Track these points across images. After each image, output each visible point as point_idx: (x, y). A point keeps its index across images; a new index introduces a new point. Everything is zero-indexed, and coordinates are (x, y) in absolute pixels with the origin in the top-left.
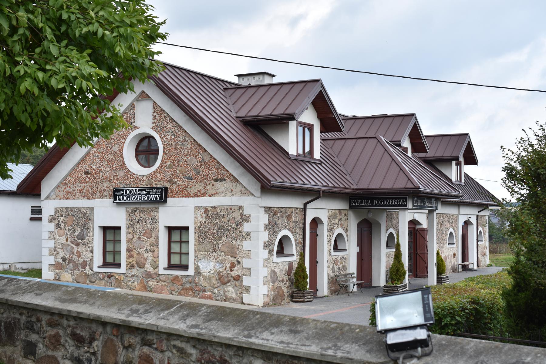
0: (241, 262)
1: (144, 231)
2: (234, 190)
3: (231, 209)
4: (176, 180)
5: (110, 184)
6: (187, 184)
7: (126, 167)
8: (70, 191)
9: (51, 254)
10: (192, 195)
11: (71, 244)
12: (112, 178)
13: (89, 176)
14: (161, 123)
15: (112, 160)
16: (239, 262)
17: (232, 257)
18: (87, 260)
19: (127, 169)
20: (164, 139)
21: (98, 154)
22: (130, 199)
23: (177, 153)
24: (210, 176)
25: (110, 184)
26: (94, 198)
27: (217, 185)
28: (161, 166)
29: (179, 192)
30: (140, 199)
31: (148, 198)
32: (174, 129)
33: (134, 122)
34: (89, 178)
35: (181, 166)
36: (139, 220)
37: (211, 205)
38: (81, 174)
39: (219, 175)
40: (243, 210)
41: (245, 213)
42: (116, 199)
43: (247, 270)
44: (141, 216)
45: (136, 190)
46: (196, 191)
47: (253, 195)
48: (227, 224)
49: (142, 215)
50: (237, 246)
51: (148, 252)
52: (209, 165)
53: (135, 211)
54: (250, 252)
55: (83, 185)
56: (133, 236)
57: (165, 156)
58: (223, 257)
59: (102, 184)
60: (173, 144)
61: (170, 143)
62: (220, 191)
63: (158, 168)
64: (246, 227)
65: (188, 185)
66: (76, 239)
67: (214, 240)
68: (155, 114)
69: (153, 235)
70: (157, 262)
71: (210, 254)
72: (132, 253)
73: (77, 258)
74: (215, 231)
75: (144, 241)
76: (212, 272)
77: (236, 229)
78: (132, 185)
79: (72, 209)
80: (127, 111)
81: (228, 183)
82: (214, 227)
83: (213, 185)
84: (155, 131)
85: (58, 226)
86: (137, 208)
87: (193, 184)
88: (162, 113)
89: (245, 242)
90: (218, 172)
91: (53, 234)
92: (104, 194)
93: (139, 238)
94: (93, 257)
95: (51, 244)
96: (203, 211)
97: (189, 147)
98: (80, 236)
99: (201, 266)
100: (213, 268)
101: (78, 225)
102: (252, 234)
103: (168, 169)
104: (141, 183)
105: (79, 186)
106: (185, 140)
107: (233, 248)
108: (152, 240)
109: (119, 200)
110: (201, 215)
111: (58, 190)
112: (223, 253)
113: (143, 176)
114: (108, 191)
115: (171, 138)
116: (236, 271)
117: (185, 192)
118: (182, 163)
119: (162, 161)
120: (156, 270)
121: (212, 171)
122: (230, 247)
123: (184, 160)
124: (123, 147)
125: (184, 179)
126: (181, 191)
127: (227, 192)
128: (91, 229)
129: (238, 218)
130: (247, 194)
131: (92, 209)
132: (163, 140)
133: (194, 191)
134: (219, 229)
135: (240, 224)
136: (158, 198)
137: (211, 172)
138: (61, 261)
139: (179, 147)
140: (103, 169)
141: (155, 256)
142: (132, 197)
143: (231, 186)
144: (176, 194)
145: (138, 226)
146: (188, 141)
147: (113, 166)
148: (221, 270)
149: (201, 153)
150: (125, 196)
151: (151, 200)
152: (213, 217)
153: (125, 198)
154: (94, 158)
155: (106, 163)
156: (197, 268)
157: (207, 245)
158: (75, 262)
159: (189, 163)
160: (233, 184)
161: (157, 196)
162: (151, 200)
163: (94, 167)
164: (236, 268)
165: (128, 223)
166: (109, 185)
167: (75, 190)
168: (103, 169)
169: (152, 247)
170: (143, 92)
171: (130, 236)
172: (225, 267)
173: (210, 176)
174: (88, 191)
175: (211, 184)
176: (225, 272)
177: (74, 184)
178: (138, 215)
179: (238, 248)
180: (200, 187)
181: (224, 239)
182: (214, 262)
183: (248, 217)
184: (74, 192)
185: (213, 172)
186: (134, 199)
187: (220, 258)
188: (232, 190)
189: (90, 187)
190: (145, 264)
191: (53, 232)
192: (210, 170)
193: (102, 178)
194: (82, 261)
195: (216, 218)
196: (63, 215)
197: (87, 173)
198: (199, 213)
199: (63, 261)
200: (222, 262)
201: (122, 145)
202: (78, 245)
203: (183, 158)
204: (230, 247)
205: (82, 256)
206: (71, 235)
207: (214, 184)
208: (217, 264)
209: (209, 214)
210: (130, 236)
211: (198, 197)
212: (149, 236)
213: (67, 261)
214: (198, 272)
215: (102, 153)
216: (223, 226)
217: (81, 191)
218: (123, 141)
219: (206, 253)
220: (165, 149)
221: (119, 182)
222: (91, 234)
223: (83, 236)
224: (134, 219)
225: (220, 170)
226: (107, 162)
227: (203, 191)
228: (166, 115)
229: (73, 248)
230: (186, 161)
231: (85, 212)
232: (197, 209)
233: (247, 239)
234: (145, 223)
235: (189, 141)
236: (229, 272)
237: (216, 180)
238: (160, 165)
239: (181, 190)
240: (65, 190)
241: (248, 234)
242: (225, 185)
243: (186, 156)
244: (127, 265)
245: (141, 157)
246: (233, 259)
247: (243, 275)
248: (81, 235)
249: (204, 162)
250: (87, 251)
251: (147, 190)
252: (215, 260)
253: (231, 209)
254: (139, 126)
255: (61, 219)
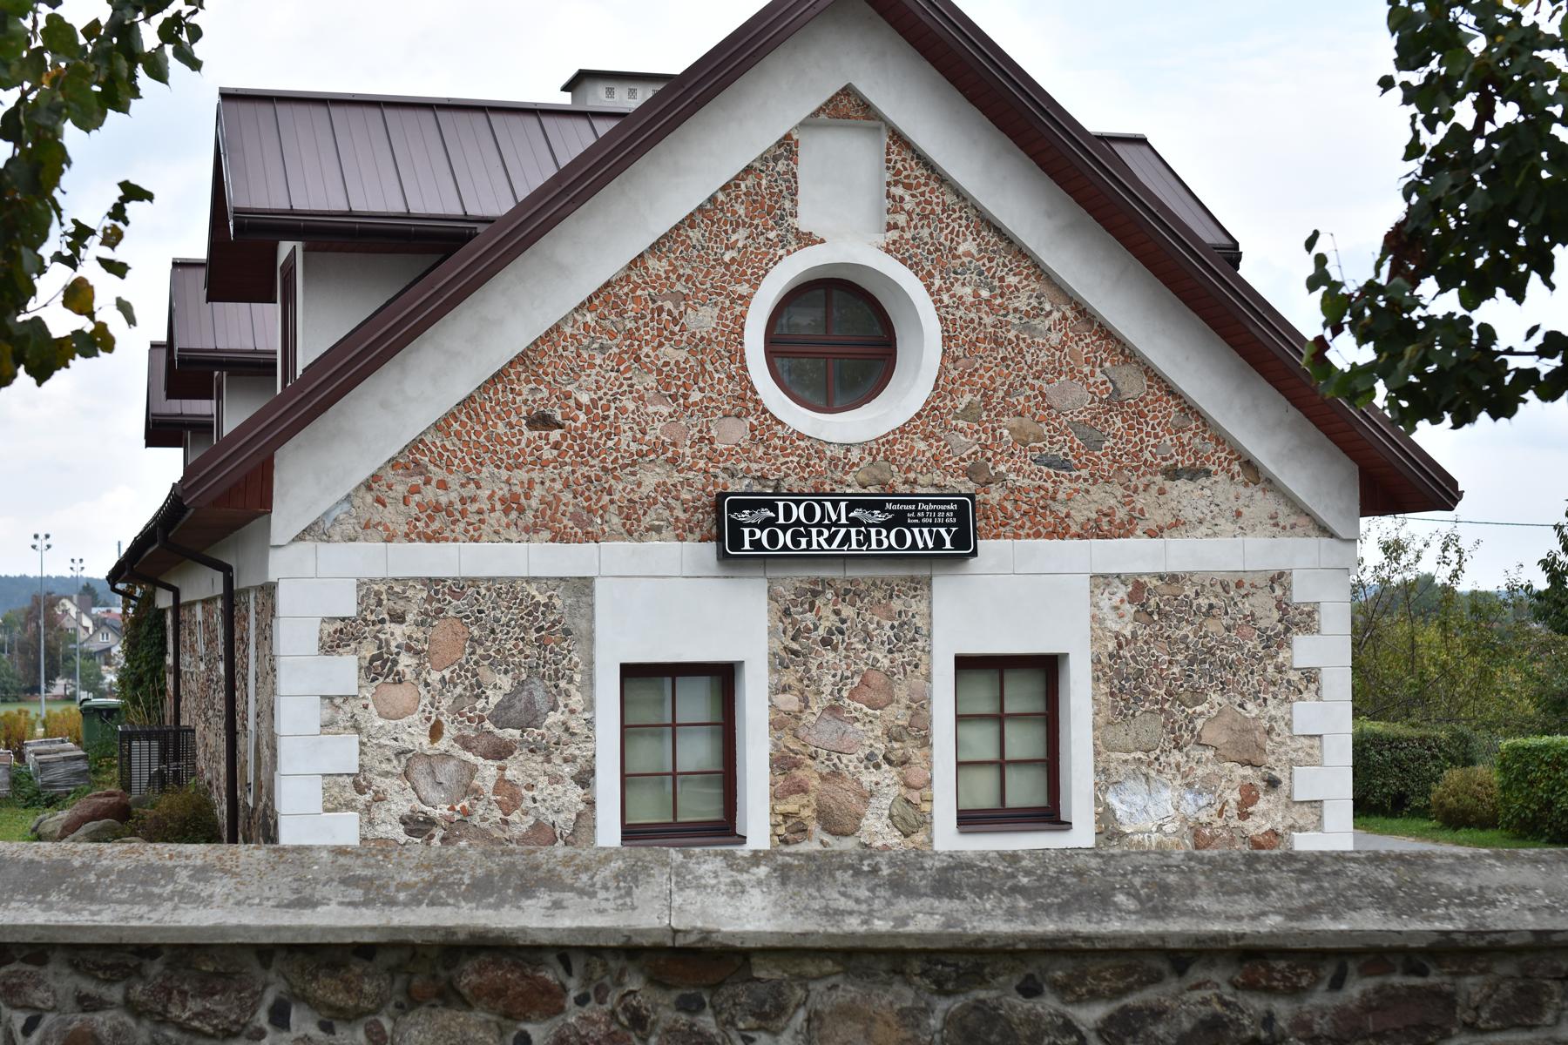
0: (1285, 781)
1: (857, 680)
2: (1244, 510)
3: (1239, 585)
4: (1002, 468)
5: (677, 477)
6: (1049, 485)
7: (758, 402)
8: (444, 500)
9: (333, 805)
10: (1075, 529)
11: (458, 751)
12: (688, 451)
13: (555, 435)
14: (925, 233)
15: (683, 370)
16: (1273, 783)
17: (1243, 764)
18: (560, 819)
19: (765, 411)
20: (945, 298)
21: (605, 339)
22: (809, 543)
23: (1004, 359)
24: (1150, 458)
25: (677, 477)
26: (590, 537)
27: (1175, 493)
28: (933, 408)
29: (1017, 516)
30: (859, 543)
31: (901, 539)
32: (991, 260)
33: (794, 215)
34: (556, 446)
35: (1021, 415)
36: (830, 632)
37: (1161, 570)
38: (510, 425)
39: (1184, 453)
40: (1287, 589)
41: (1297, 597)
42: (737, 542)
43: (1306, 808)
44: (844, 614)
45: (835, 504)
46: (1094, 516)
47: (1325, 531)
48: (1222, 642)
49: (847, 611)
50: (1265, 723)
51: (877, 766)
52: (1141, 414)
53: (815, 594)
54: (1316, 742)
55: (521, 475)
56: (805, 701)
57: (950, 366)
58: (1210, 768)
59: (633, 474)
60: (988, 320)
61: (972, 315)
62: (1188, 514)
63: (918, 415)
64: (1303, 651)
65: (1055, 492)
66: (488, 725)
67: (1173, 705)
68: (898, 191)
69: (902, 693)
70: (925, 807)
71: (1157, 759)
72: (799, 774)
73: (498, 814)
74: (1176, 669)
75: (856, 719)
76: (1168, 828)
77: (1261, 659)
78: (791, 482)
79: (458, 587)
80: (757, 165)
81: (1219, 488)
82: (1173, 655)
83: (1162, 492)
84: (903, 261)
85: (380, 668)
86: (828, 583)
87: (1074, 486)
88: (932, 191)
89: (1298, 706)
90: (1182, 445)
91: (347, 708)
92: (647, 521)
93: (834, 710)
94: (591, 803)
95: (343, 754)
96: (1122, 592)
97: (1055, 337)
98: (512, 713)
99: (1121, 810)
100: (1172, 812)
101: (499, 662)
102: (1326, 678)
103: (961, 424)
104: (838, 475)
105: (493, 482)
106: (1038, 312)
107: (1247, 731)
108: (897, 714)
109: (756, 544)
110: (1116, 608)
111: (369, 498)
112: (1210, 753)
113: (848, 447)
114: (668, 506)
115: (976, 295)
116: (1265, 815)
117: (1043, 516)
118: (1022, 399)
119: (936, 387)
120: (919, 837)
121: (1156, 436)
122: (1237, 727)
123: (1032, 388)
124: (743, 315)
125: (1034, 466)
126: (1025, 513)
127: (1220, 521)
128: (577, 678)
129: (1270, 619)
130: (1297, 530)
131: (583, 587)
132: (938, 302)
133: (1082, 512)
134: (1191, 663)
135: (1276, 641)
136: (948, 539)
137: (1153, 441)
138: (399, 833)
139: (1011, 335)
140: (631, 406)
141: (915, 781)
142: (820, 534)
143: (1232, 498)
144: (1004, 526)
145: (830, 656)
146: (1050, 313)
147: (685, 397)
148: (1204, 818)
149: (1107, 365)
150: (784, 528)
151: (914, 545)
152: (1164, 615)
153: (785, 538)
154: (585, 355)
155: (651, 380)
156: (1105, 817)
157: (1148, 726)
158: (484, 834)
159: (1056, 401)
160: (1241, 489)
161: (943, 531)
162: (914, 545)
163: (585, 398)
164: (1262, 805)
165: (778, 647)
166: (670, 482)
167: (473, 500)
168: (631, 406)
169: (896, 745)
170: (848, 91)
171: (789, 701)
172: (1218, 806)
173: (1150, 458)
174: (552, 503)
175: (1154, 489)
176: (1220, 822)
177: (468, 469)
178: (827, 612)
179: (1269, 732)
180: (1105, 497)
181: (1215, 697)
182: (1174, 789)
183: (1310, 614)
184: (475, 507)
185: (1165, 445)
186: (830, 541)
187: (1200, 771)
188: (1239, 514)
189: (567, 485)
190: (859, 817)
191: (346, 698)
192: (1148, 434)
193: (634, 447)
194: (524, 828)
195: (1180, 620)
196: (410, 617)
197: (542, 421)
198: (1105, 603)
199: (409, 832)
200: (1208, 785)
201: (738, 310)
202: (500, 752)
203: (1030, 380)
204: (1237, 727)
205: (528, 803)
206: (457, 710)
207: (1167, 488)
208: (1189, 797)
209: (1152, 602)
210: (790, 702)
211: (1098, 537)
212: (883, 697)
213: (439, 833)
214: (1108, 827)
215: (630, 334)
216: (1210, 651)
217: (512, 504)
218: (744, 289)
219: (1139, 754)
220: (950, 338)
221: (725, 469)
222: (576, 700)
223: (526, 709)
224: (808, 630)
225: (1190, 434)
226: (654, 376)
227: (1121, 514)
228: (950, 199)
229: (473, 770)
230: (1044, 395)
231: (542, 599)
232: (1097, 586)
233: (1305, 695)
234: (859, 646)
235: (1056, 315)
236: (1234, 822)
237: (1173, 474)
238: (927, 403)
239: (1025, 507)
240: (417, 497)
241: (1311, 676)
242: (1207, 492)
243: (1040, 372)
244: (774, 826)
245: (778, 362)
246: (1248, 771)
247: (1292, 827)
248: (519, 706)
249: (1121, 404)
250: (555, 779)
251: (889, 506)
252: (1178, 781)
253: (1239, 585)
254: (818, 234)
255: (397, 633)
